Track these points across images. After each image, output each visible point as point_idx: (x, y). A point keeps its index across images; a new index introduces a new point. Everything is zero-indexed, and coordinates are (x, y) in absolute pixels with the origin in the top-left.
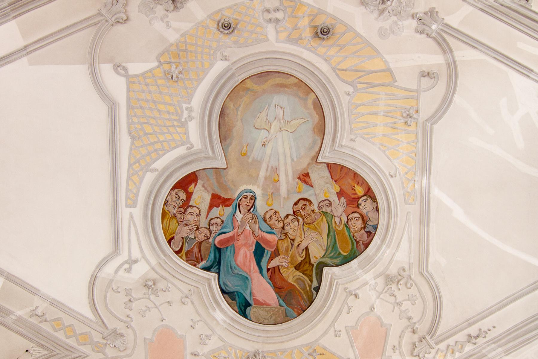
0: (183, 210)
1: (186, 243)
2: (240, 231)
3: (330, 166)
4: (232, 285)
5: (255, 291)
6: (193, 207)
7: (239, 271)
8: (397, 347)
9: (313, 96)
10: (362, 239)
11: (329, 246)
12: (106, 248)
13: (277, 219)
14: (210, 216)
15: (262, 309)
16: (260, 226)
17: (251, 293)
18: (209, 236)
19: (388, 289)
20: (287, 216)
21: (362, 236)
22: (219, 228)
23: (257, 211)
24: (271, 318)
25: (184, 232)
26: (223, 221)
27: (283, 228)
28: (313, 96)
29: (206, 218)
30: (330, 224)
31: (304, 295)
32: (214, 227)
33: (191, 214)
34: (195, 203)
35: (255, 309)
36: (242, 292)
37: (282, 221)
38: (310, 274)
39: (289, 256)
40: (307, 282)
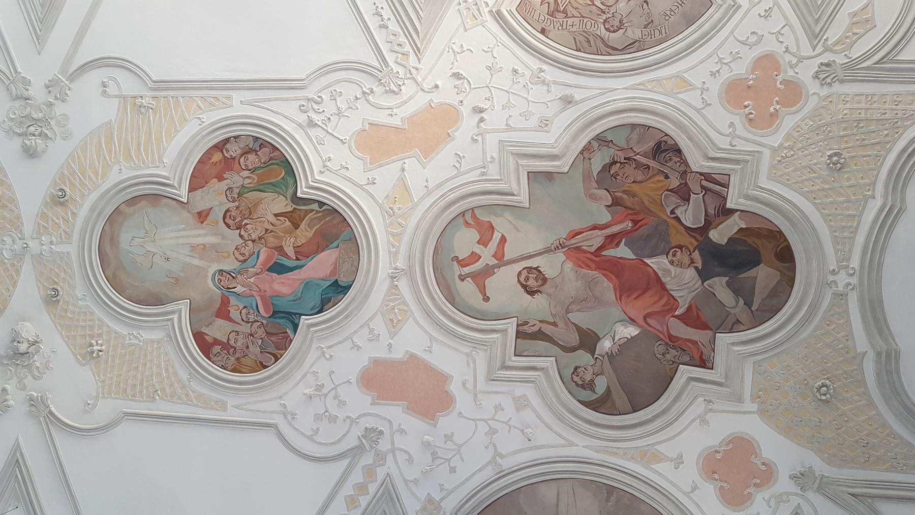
0: (233, 350)
1: (266, 349)
2: (256, 289)
3: (191, 189)
4: (314, 299)
5: (321, 275)
6: (229, 338)
7: (299, 291)
8: (389, 112)
9: (123, 207)
10: (268, 154)
11: (274, 190)
12: (270, 437)
13: (243, 248)
14: (240, 321)
15: (340, 268)
16: (251, 266)
17: (323, 280)
18: (260, 323)
19: (323, 123)
20: (241, 236)
21: (264, 154)
22: (251, 311)
23: (235, 269)
24: (351, 257)
25: (255, 350)
26: (245, 307)
27: (253, 241)
28: (123, 207)
29: (241, 325)
30: (251, 189)
31: (327, 219)
32: (251, 317)
33: (236, 340)
34: (224, 336)
35: (342, 276)
36: (321, 289)
37: (246, 242)
38: (304, 211)
39: (283, 235)
40: (314, 215)
